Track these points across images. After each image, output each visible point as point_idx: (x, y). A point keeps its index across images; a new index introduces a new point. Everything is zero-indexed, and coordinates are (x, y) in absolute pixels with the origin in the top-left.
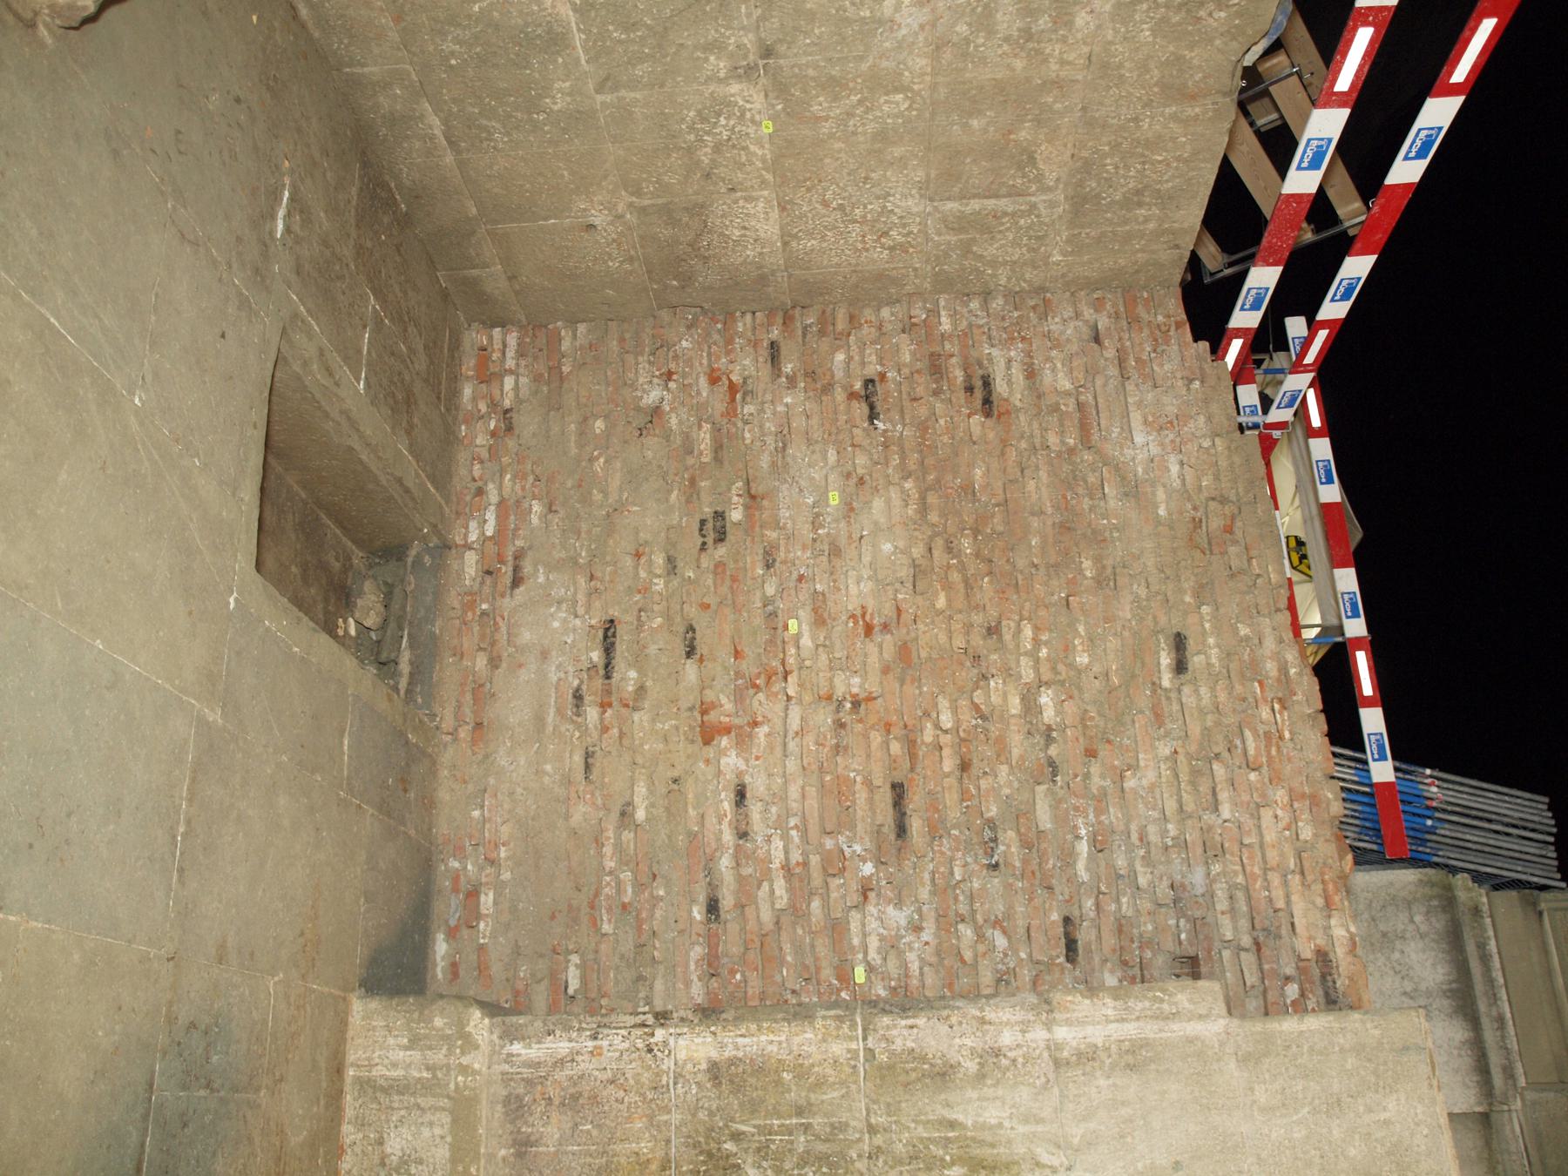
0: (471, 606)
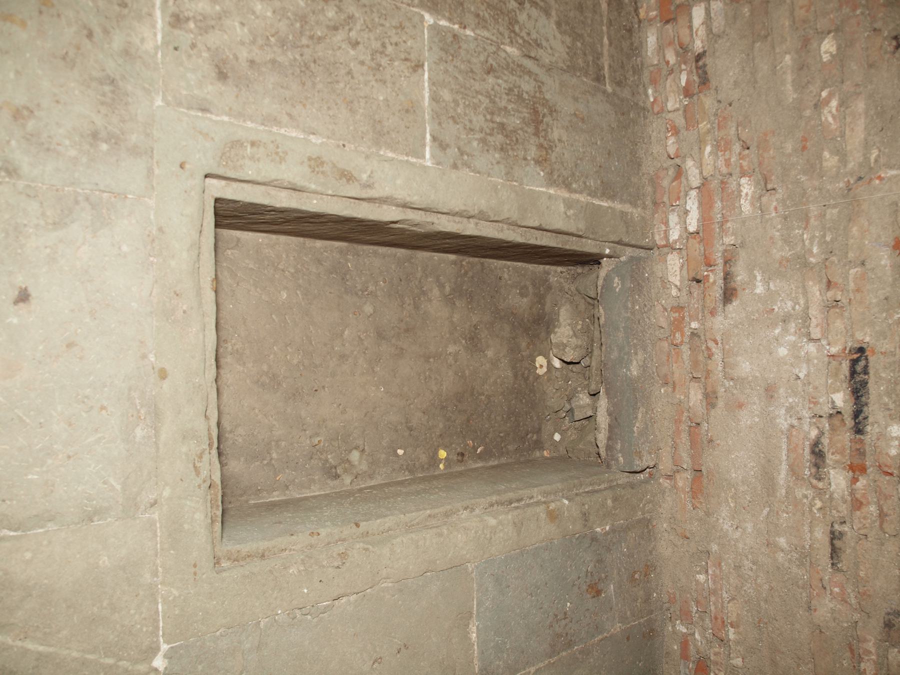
0: (677, 325)
